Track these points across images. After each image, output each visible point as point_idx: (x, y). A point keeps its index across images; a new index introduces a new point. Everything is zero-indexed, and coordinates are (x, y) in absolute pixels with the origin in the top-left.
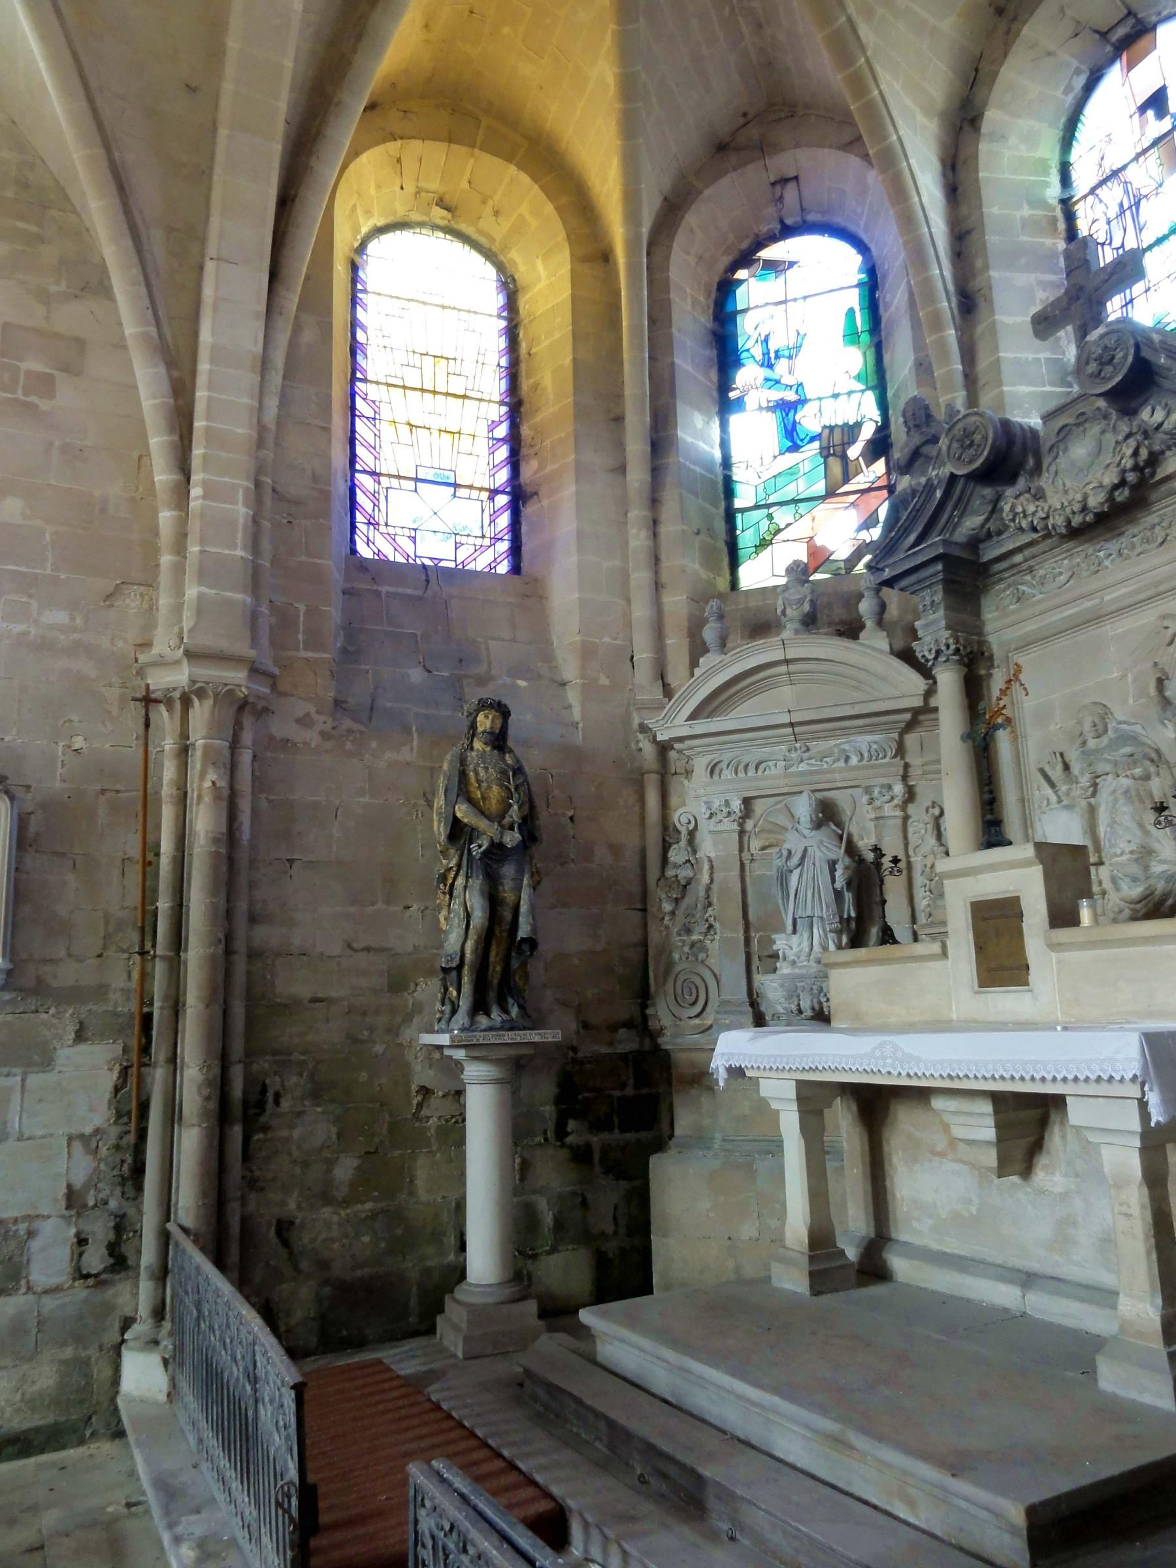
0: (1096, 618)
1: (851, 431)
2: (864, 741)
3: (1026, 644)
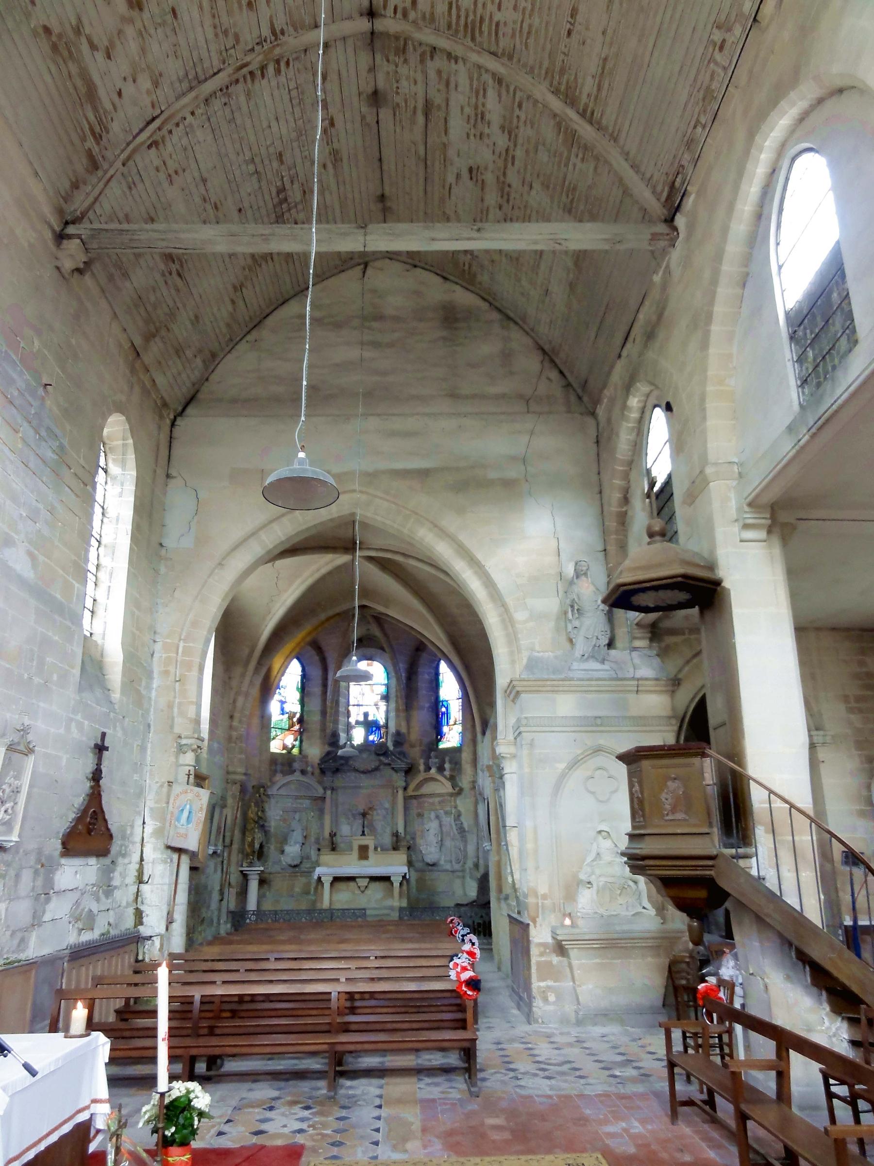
0: (360, 787)
1: (295, 714)
3: (345, 788)
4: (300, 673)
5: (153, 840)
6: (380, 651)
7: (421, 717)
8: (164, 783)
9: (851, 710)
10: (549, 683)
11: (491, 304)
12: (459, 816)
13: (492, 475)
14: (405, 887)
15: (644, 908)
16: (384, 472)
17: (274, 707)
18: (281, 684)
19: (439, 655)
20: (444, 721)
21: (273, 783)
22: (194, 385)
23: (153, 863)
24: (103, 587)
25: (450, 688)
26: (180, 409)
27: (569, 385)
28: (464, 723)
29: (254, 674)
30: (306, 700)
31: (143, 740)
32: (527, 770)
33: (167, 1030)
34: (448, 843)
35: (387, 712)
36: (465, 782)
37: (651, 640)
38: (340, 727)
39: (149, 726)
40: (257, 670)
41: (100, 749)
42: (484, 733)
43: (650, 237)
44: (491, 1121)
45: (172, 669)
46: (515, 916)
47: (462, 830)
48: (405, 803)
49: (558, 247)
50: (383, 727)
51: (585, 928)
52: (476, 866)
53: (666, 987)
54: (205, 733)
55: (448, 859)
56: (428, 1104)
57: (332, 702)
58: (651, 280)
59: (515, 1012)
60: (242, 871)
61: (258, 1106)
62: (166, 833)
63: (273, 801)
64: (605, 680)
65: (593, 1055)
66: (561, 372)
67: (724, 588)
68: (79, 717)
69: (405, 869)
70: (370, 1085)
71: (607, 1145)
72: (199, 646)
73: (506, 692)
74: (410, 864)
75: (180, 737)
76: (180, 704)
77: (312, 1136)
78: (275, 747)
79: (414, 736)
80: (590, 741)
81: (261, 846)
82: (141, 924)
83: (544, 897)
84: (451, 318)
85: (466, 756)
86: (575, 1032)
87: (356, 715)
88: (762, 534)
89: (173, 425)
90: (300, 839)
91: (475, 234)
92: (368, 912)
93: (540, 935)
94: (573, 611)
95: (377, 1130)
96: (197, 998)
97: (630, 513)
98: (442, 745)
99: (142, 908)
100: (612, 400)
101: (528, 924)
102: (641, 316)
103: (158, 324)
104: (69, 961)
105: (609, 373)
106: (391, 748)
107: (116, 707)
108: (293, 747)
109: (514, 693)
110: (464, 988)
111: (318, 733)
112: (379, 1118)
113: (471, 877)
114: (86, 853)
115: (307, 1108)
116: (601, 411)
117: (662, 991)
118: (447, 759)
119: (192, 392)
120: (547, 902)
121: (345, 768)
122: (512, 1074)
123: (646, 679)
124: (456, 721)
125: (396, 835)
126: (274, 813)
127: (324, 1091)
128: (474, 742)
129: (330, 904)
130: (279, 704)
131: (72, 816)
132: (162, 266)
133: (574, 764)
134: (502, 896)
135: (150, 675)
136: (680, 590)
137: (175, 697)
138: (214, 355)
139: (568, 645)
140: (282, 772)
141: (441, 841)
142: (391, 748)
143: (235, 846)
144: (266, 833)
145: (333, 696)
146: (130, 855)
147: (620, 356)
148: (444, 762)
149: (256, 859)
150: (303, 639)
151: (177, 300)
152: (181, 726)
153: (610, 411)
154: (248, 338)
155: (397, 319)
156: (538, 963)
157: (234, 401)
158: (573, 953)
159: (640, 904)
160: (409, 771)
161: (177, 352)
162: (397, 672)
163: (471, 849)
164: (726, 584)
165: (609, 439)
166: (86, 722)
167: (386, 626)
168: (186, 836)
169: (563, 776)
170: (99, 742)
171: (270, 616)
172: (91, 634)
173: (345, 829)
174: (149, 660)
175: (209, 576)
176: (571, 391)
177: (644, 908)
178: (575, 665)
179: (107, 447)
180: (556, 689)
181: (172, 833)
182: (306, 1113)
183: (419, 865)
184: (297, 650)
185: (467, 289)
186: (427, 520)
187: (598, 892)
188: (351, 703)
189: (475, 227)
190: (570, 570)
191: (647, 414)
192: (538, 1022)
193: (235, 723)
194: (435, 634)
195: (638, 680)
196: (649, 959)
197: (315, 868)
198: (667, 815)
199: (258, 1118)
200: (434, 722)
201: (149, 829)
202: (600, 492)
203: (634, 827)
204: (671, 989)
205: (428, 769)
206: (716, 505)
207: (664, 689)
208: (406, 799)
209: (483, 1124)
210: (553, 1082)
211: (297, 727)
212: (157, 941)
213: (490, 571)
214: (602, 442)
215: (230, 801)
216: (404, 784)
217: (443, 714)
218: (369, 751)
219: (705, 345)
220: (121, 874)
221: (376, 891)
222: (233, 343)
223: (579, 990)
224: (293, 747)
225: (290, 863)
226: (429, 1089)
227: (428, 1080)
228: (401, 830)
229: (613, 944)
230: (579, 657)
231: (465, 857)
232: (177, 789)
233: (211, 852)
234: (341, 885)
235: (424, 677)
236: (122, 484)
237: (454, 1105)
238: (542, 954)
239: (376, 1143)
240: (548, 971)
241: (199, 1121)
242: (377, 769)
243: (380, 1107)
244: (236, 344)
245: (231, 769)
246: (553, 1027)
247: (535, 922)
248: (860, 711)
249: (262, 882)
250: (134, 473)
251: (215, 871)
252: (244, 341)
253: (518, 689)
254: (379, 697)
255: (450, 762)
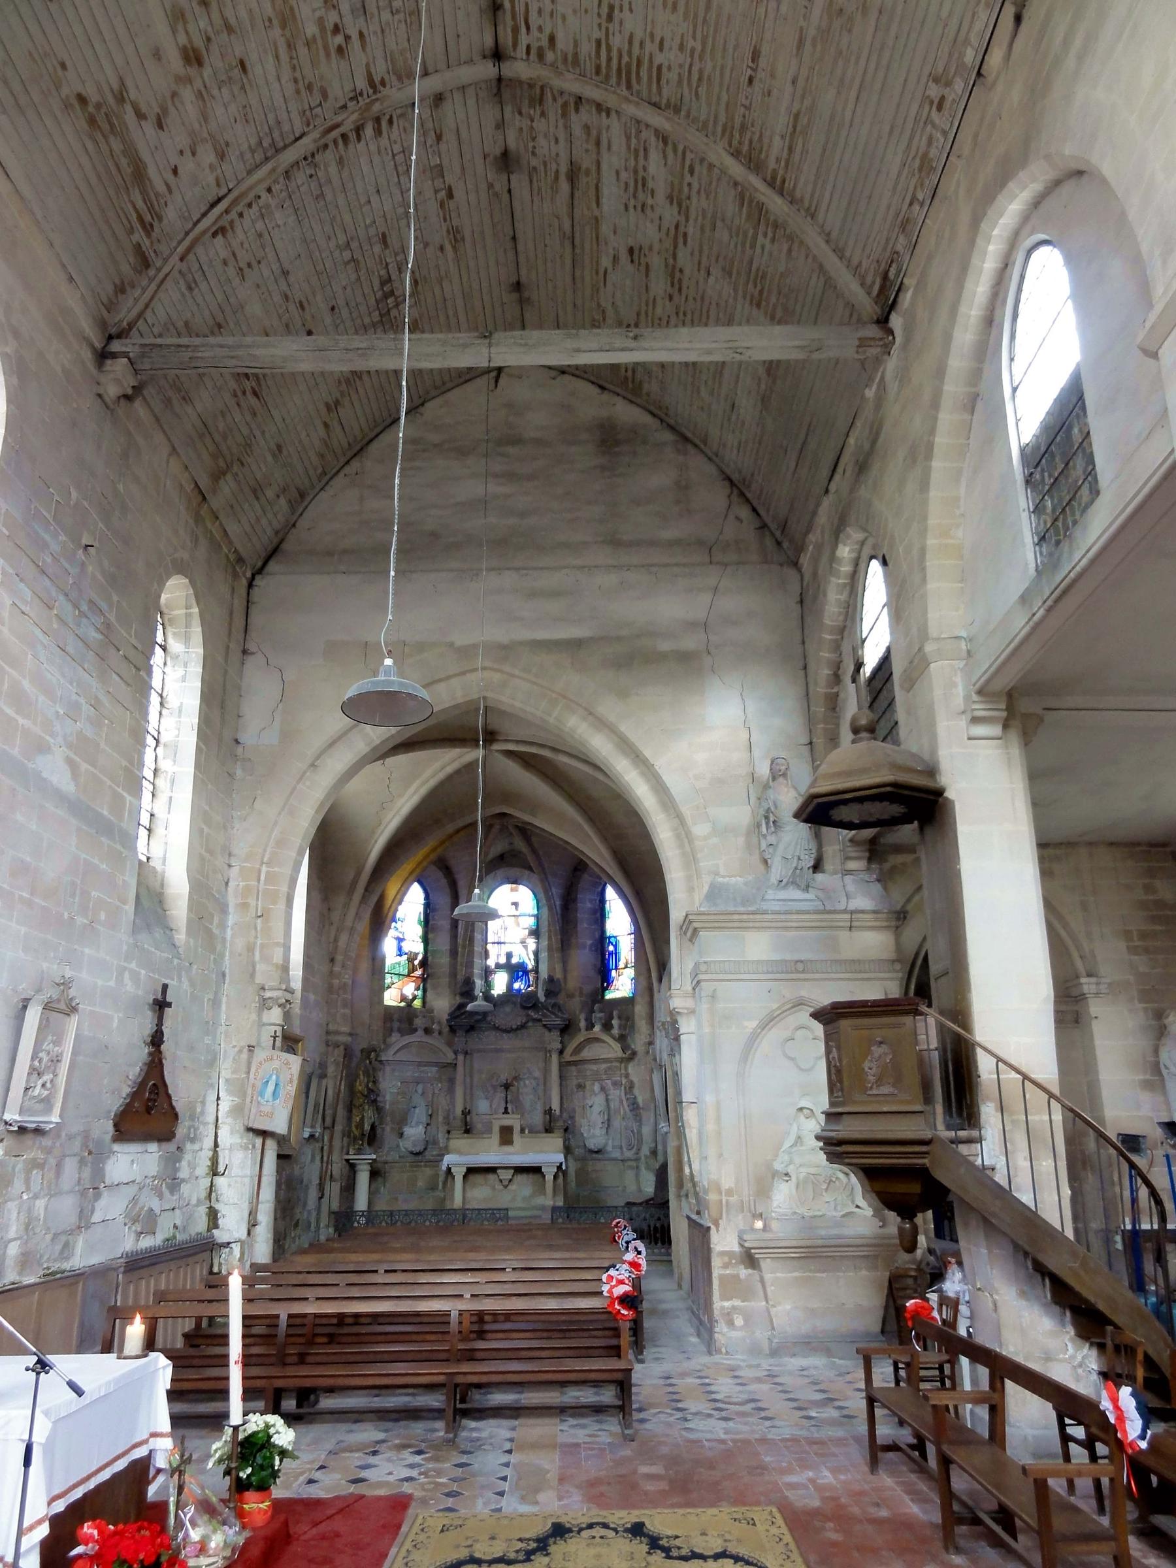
1: (416, 955)
2: (434, 1069)
3: (479, 1051)
4: (423, 901)
5: (229, 1120)
6: (527, 872)
7: (582, 958)
8: (243, 1047)
9: (1132, 950)
10: (736, 917)
11: (662, 421)
12: (631, 1086)
13: (665, 646)
14: (560, 1180)
15: (857, 1207)
16: (521, 643)
17: (388, 946)
18: (398, 915)
19: (605, 878)
20: (612, 964)
21: (388, 1046)
22: (277, 533)
23: (231, 1149)
24: (162, 798)
25: (619, 920)
26: (260, 564)
27: (764, 526)
28: (636, 967)
29: (361, 903)
30: (430, 936)
31: (216, 993)
32: (707, 1030)
33: (240, 1351)
34: (617, 1123)
35: (536, 954)
36: (638, 1042)
37: (870, 860)
38: (476, 971)
39: (224, 975)
40: (364, 899)
41: (161, 1005)
42: (660, 980)
43: (857, 343)
44: (644, 1469)
45: (252, 902)
46: (694, 1217)
47: (635, 1106)
48: (560, 1070)
49: (738, 357)
50: (531, 971)
51: (782, 1232)
52: (654, 1153)
53: (886, 1308)
54: (297, 984)
55: (617, 1143)
56: (572, 1448)
57: (464, 940)
58: (863, 396)
59: (694, 1340)
60: (347, 1161)
61: (358, 1450)
62: (246, 1112)
63: (388, 1069)
64: (808, 912)
65: (786, 1392)
66: (754, 510)
67: (947, 799)
68: (133, 965)
69: (560, 1158)
70: (498, 1427)
71: (787, 1497)
72: (287, 871)
73: (681, 928)
74: (568, 1150)
75: (263, 988)
76: (262, 946)
77: (422, 1485)
78: (391, 998)
79: (572, 984)
80: (789, 992)
81: (373, 1127)
82: (216, 1227)
83: (730, 1192)
84: (610, 440)
85: (640, 1009)
86: (766, 1363)
87: (495, 956)
88: (996, 730)
89: (250, 585)
90: (424, 1119)
91: (633, 344)
92: (511, 1214)
93: (724, 1241)
94: (767, 823)
95: (504, 1479)
96: (284, 1317)
97: (842, 695)
98: (609, 996)
99: (217, 1206)
100: (819, 547)
101: (709, 1228)
102: (851, 441)
103: (228, 458)
104: (124, 1273)
105: (814, 513)
106: (542, 998)
107: (181, 950)
108: (415, 998)
109: (691, 932)
110: (617, 1307)
111: (445, 980)
112: (507, 1465)
113: (648, 1168)
114: (147, 1137)
115: (420, 1453)
116: (805, 560)
117: (881, 1313)
118: (615, 1013)
119: (276, 541)
120: (733, 1199)
121: (483, 1025)
122: (679, 1415)
123: (863, 912)
124: (627, 963)
125: (549, 1112)
126: (390, 1085)
127: (442, 1434)
128: (650, 990)
129: (464, 1203)
130: (395, 943)
131: (126, 1090)
132: (233, 384)
133: (769, 1021)
134: (683, 1193)
135: (224, 910)
136: (892, 802)
137: (256, 937)
138: (302, 495)
139: (762, 867)
140: (400, 1030)
141: (609, 1120)
142: (542, 998)
143: (339, 1128)
144: (379, 1110)
145: (466, 931)
146: (201, 1140)
147: (827, 491)
148: (611, 1018)
149: (366, 1145)
150: (425, 858)
151: (253, 426)
152: (265, 974)
153: (816, 560)
154: (347, 470)
155: (538, 442)
156: (721, 1277)
157: (330, 554)
158: (765, 1265)
159: (853, 1202)
160: (567, 1029)
161: (254, 491)
162: (549, 898)
163: (646, 1130)
164: (950, 794)
165: (815, 598)
166: (143, 972)
167: (534, 839)
168: (271, 1115)
169: (753, 1040)
170: (160, 997)
171: (382, 827)
172: (148, 858)
173: (483, 1106)
174: (223, 889)
175: (298, 782)
176: (767, 533)
177: (857, 1207)
178: (770, 894)
179: (166, 617)
180: (745, 925)
181: (253, 1111)
182: (418, 1459)
183: (578, 1152)
184: (418, 871)
185: (631, 402)
186: (578, 704)
187: (797, 1187)
188: (490, 939)
189: (631, 334)
190: (764, 770)
191: (862, 566)
192: (721, 1353)
193: (337, 969)
194: (597, 852)
195: (852, 912)
196: (864, 1272)
197: (443, 1155)
198: (871, 1088)
199: (359, 1464)
200: (599, 963)
201: (224, 1106)
202: (805, 668)
203: (832, 1104)
204: (892, 1311)
205: (590, 1026)
206: (938, 693)
207: (885, 924)
208: (563, 1066)
209: (635, 1472)
210: (731, 1424)
211: (419, 972)
212: (236, 1249)
213: (660, 771)
214: (807, 601)
215: (331, 1070)
216: (560, 1046)
217: (611, 954)
218: (514, 1003)
219: (924, 486)
220: (189, 1162)
221: (523, 1187)
222: (326, 477)
223: (773, 1311)
224: (415, 998)
225: (411, 1149)
226: (572, 1431)
227: (572, 1421)
228: (556, 1106)
229: (816, 1253)
230: (776, 883)
231: (640, 1141)
232: (260, 1055)
233: (306, 1135)
234: (477, 1178)
235: (585, 904)
236: (185, 665)
237: (602, 1450)
238: (726, 1266)
239: (501, 1494)
240: (733, 1287)
241: (281, 1461)
242: (523, 1026)
243: (510, 1452)
244: (331, 478)
245: (331, 1027)
246: (739, 1359)
247: (717, 1225)
248: (1147, 950)
249: (375, 1174)
250: (201, 651)
251: (313, 1160)
252: (341, 474)
253: (695, 925)
254: (527, 932)
255: (620, 1018)
